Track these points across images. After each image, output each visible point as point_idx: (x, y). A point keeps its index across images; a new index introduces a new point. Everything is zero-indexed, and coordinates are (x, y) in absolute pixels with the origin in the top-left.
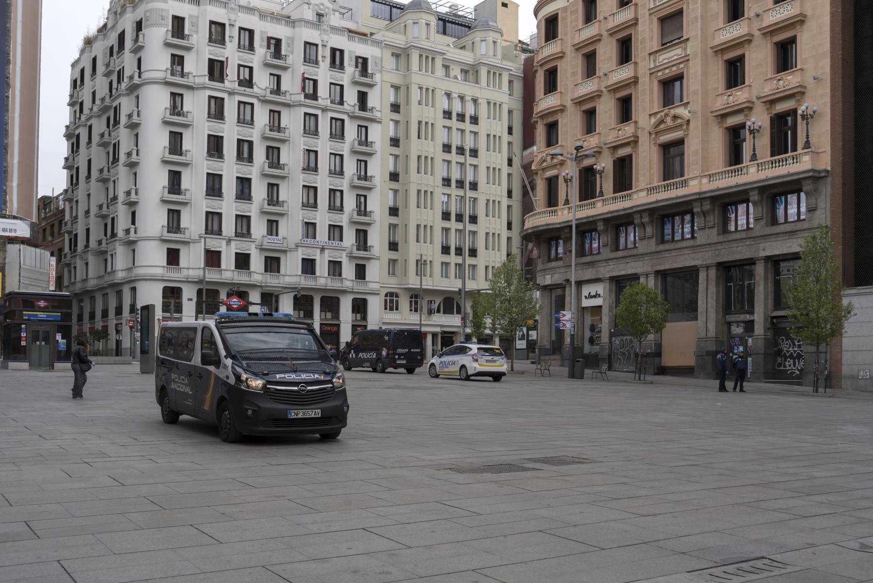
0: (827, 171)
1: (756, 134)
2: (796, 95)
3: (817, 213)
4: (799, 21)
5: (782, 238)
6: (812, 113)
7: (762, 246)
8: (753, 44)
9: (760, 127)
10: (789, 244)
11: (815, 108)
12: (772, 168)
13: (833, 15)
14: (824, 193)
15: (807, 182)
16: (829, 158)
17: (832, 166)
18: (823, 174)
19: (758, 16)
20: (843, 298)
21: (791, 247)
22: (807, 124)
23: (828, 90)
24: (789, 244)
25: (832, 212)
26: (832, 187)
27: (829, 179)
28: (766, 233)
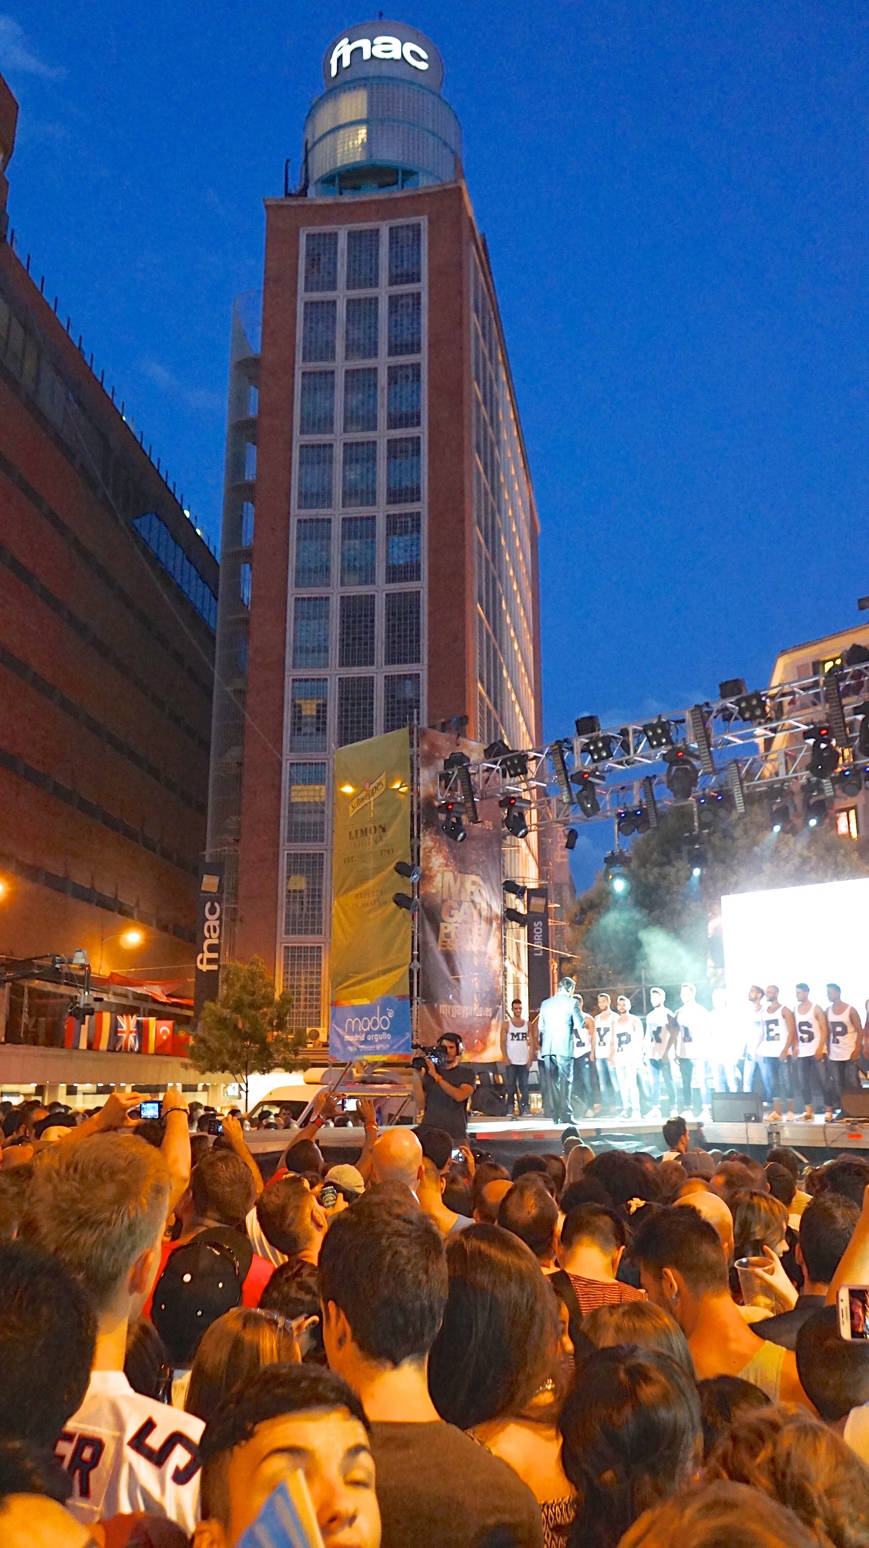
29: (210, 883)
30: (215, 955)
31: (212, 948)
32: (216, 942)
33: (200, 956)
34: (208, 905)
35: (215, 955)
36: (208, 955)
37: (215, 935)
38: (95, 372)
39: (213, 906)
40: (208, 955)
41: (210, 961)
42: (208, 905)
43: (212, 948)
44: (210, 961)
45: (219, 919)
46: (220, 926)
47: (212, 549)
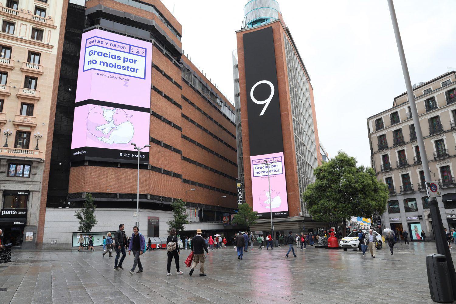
0: (44, 160)
1: (9, 136)
2: (33, 127)
3: (37, 176)
4: (38, 100)
5: (16, 183)
6: (40, 136)
7: (3, 185)
8: (9, 98)
9: (11, 134)
10: (19, 186)
11: (42, 135)
12: (21, 153)
13: (52, 104)
14: (41, 168)
15: (36, 163)
16: (45, 156)
17: (45, 159)
18: (42, 161)
19: (15, 88)
20: (46, 212)
21: (21, 187)
22: (38, 140)
23: (47, 130)
24: (19, 186)
25: (44, 177)
26: (45, 167)
27: (44, 164)
28: (6, 179)
29: (239, 185)
30: (241, 201)
31: (241, 199)
32: (241, 197)
33: (238, 201)
34: (239, 190)
35: (241, 201)
36: (240, 201)
37: (241, 196)
38: (201, 71)
39: (240, 189)
40: (240, 201)
41: (240, 202)
42: (239, 190)
43: (241, 199)
44: (240, 202)
45: (241, 192)
46: (242, 194)
47: (233, 104)
